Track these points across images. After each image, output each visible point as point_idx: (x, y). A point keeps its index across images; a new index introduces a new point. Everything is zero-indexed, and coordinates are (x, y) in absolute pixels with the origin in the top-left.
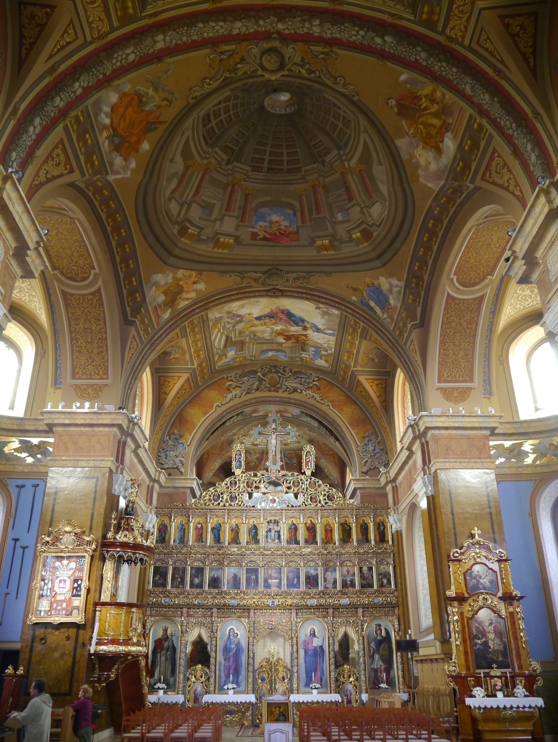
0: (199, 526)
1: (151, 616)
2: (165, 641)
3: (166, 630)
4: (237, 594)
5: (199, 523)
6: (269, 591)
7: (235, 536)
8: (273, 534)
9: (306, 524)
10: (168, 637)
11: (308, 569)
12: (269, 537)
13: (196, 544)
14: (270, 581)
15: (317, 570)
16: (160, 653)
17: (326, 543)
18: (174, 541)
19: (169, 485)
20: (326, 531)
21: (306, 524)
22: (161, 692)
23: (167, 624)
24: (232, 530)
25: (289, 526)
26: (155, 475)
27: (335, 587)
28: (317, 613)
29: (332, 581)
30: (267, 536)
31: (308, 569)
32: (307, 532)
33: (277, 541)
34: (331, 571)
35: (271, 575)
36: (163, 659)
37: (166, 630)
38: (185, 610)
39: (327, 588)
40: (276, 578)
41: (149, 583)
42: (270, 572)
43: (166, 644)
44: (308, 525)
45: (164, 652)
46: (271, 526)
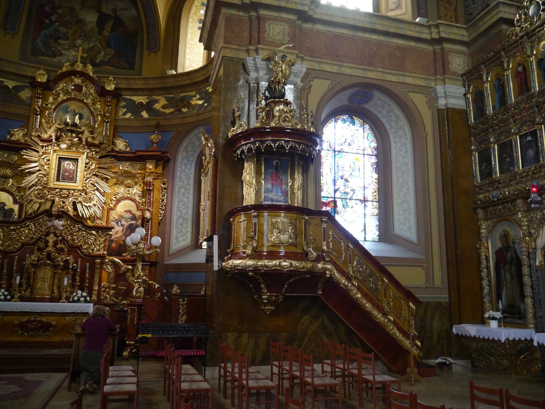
0: (520, 69)
1: (486, 219)
2: (507, 251)
3: (505, 236)
5: (519, 65)
10: (509, 246)
13: (520, 98)
16: (504, 268)
18: (494, 108)
19: (474, 35)
22: (494, 324)
23: (503, 227)
26: (431, 34)
36: (508, 276)
37: (505, 236)
38: (519, 202)
41: (474, 177)
43: (509, 256)
45: (508, 267)
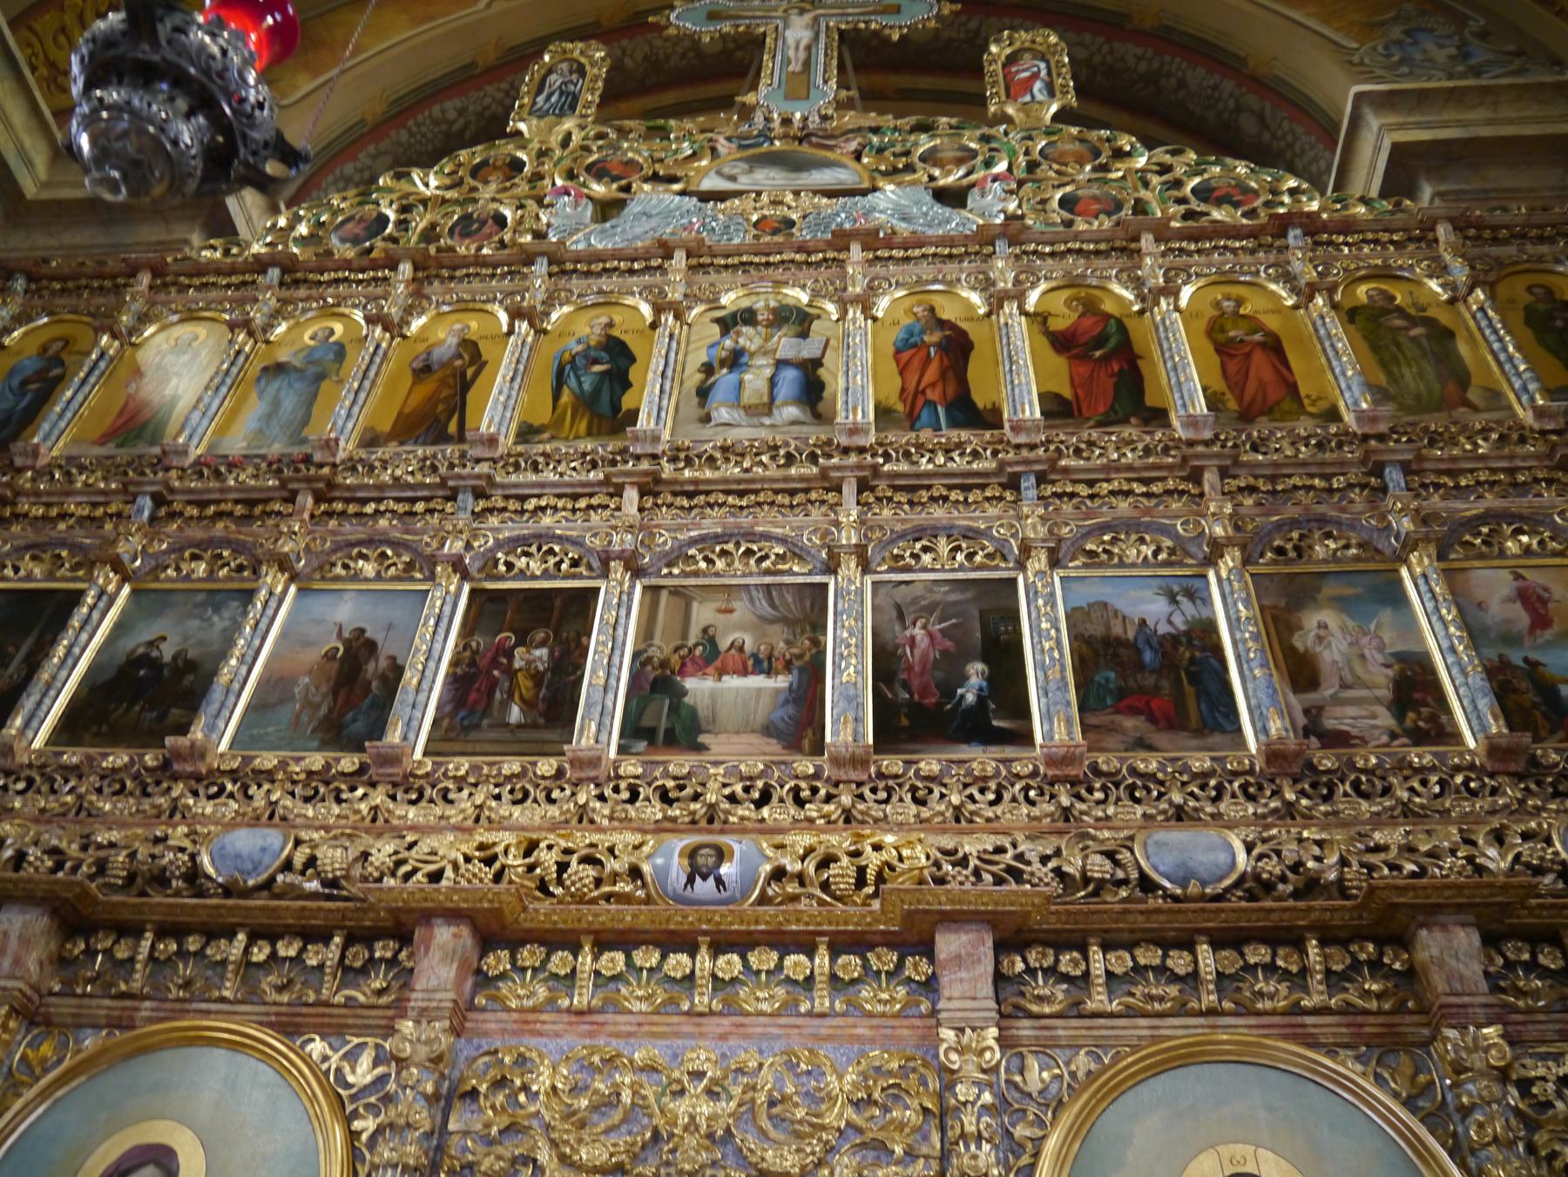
4: (319, 785)
6: (680, 763)
7: (432, 400)
8: (755, 380)
9: (1039, 319)
11: (1097, 588)
12: (718, 394)
14: (698, 687)
15: (1197, 594)
17: (1246, 416)
20: (1225, 349)
21: (1039, 319)
24: (424, 370)
25: (892, 336)
27: (1440, 732)
28: (1274, 993)
29: (1381, 678)
30: (703, 393)
31: (1097, 588)
32: (1059, 363)
33: (792, 412)
34: (1342, 604)
35: (709, 637)
39: (1335, 740)
40: (762, 664)
42: (703, 614)
44: (1057, 324)
46: (749, 338)
